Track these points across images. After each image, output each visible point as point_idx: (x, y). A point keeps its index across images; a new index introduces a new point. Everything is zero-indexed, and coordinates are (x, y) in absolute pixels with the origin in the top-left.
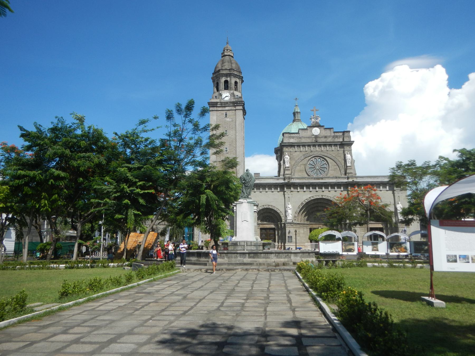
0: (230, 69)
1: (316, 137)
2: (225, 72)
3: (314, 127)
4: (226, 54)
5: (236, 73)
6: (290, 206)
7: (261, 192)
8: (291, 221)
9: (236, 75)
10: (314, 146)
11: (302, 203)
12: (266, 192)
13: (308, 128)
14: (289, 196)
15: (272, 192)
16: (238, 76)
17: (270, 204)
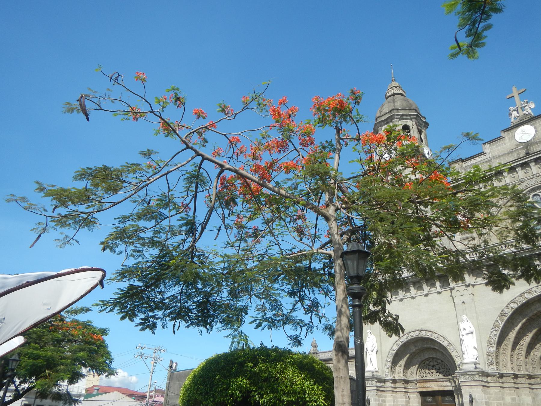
0: (390, 111)
1: (527, 145)
2: (383, 119)
3: (517, 126)
4: (388, 95)
5: (401, 113)
6: (467, 325)
7: (401, 300)
8: (471, 367)
9: (402, 115)
10: (525, 165)
11: (502, 314)
12: (413, 298)
13: (503, 135)
14: (463, 299)
15: (426, 295)
16: (406, 115)
17: (423, 327)
